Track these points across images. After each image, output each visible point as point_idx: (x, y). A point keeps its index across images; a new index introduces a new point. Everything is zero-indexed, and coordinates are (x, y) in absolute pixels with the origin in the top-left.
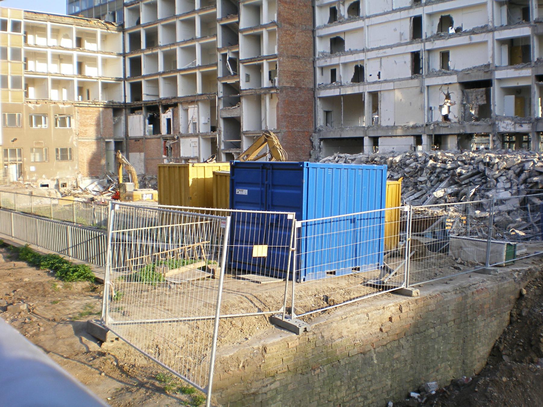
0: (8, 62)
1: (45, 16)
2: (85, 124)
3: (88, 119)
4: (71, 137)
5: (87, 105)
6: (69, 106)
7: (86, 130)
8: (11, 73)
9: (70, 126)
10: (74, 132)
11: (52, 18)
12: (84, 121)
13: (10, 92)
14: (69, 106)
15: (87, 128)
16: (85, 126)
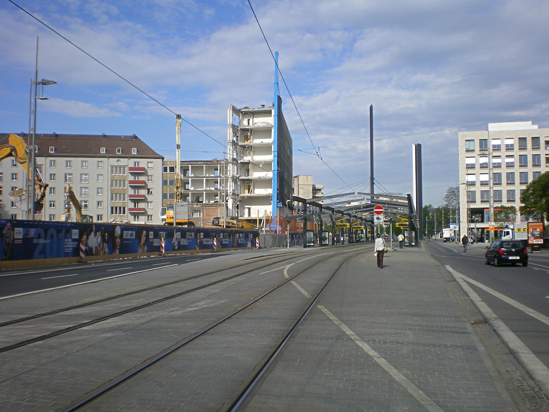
0: (168, 186)
1: (188, 162)
2: (209, 215)
3: (211, 212)
4: (200, 222)
5: (211, 205)
6: (199, 206)
7: (210, 218)
8: (169, 192)
9: (200, 216)
10: (202, 219)
11: (191, 163)
12: (208, 213)
13: (168, 201)
14: (199, 206)
15: (210, 217)
16: (209, 216)
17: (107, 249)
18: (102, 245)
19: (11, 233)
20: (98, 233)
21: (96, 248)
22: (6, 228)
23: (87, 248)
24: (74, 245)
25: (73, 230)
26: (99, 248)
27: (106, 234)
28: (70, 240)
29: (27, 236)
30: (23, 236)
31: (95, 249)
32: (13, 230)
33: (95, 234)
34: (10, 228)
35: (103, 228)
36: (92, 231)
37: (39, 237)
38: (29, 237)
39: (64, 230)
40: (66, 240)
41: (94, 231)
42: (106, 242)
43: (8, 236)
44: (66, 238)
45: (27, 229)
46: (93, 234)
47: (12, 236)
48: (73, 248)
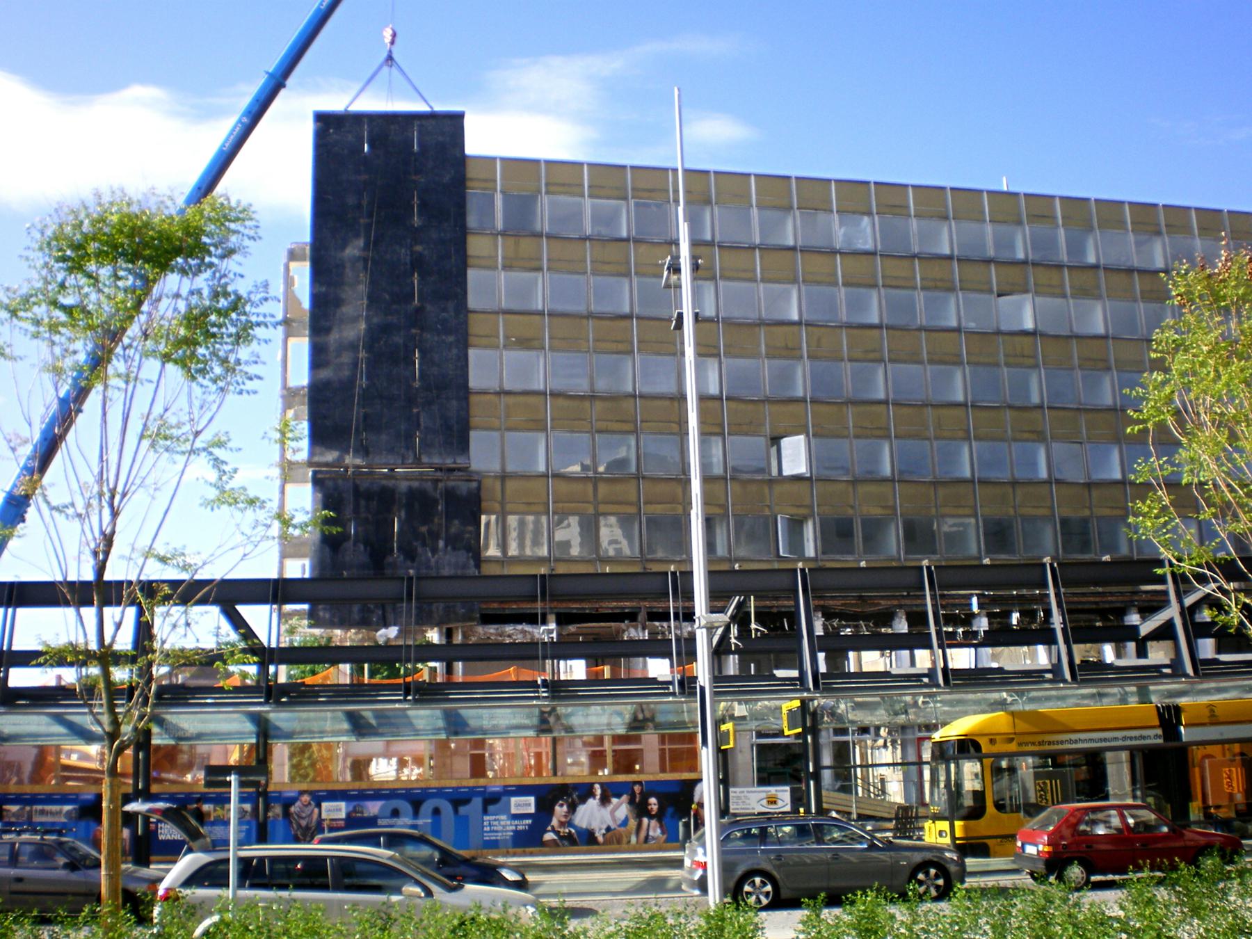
17: (659, 831)
18: (633, 823)
19: (312, 812)
20: (615, 800)
21: (608, 829)
22: (298, 804)
23: (573, 831)
24: (516, 826)
25: (514, 800)
26: (622, 829)
27: (653, 800)
28: (503, 817)
29: (359, 815)
30: (348, 815)
31: (604, 831)
32: (319, 806)
33: (605, 800)
34: (310, 804)
35: (637, 788)
36: (593, 795)
37: (395, 813)
38: (365, 815)
39: (477, 802)
40: (486, 818)
41: (598, 797)
42: (651, 817)
43: (304, 815)
44: (485, 812)
45: (355, 803)
46: (593, 803)
47: (315, 816)
48: (512, 831)
